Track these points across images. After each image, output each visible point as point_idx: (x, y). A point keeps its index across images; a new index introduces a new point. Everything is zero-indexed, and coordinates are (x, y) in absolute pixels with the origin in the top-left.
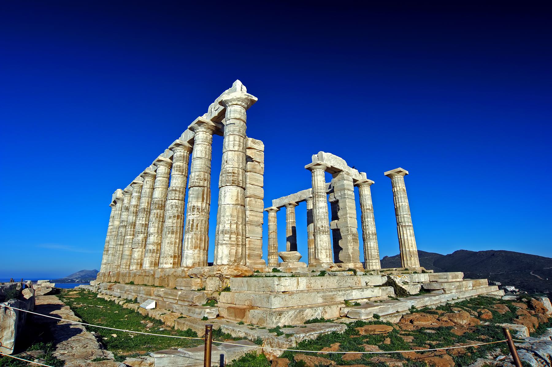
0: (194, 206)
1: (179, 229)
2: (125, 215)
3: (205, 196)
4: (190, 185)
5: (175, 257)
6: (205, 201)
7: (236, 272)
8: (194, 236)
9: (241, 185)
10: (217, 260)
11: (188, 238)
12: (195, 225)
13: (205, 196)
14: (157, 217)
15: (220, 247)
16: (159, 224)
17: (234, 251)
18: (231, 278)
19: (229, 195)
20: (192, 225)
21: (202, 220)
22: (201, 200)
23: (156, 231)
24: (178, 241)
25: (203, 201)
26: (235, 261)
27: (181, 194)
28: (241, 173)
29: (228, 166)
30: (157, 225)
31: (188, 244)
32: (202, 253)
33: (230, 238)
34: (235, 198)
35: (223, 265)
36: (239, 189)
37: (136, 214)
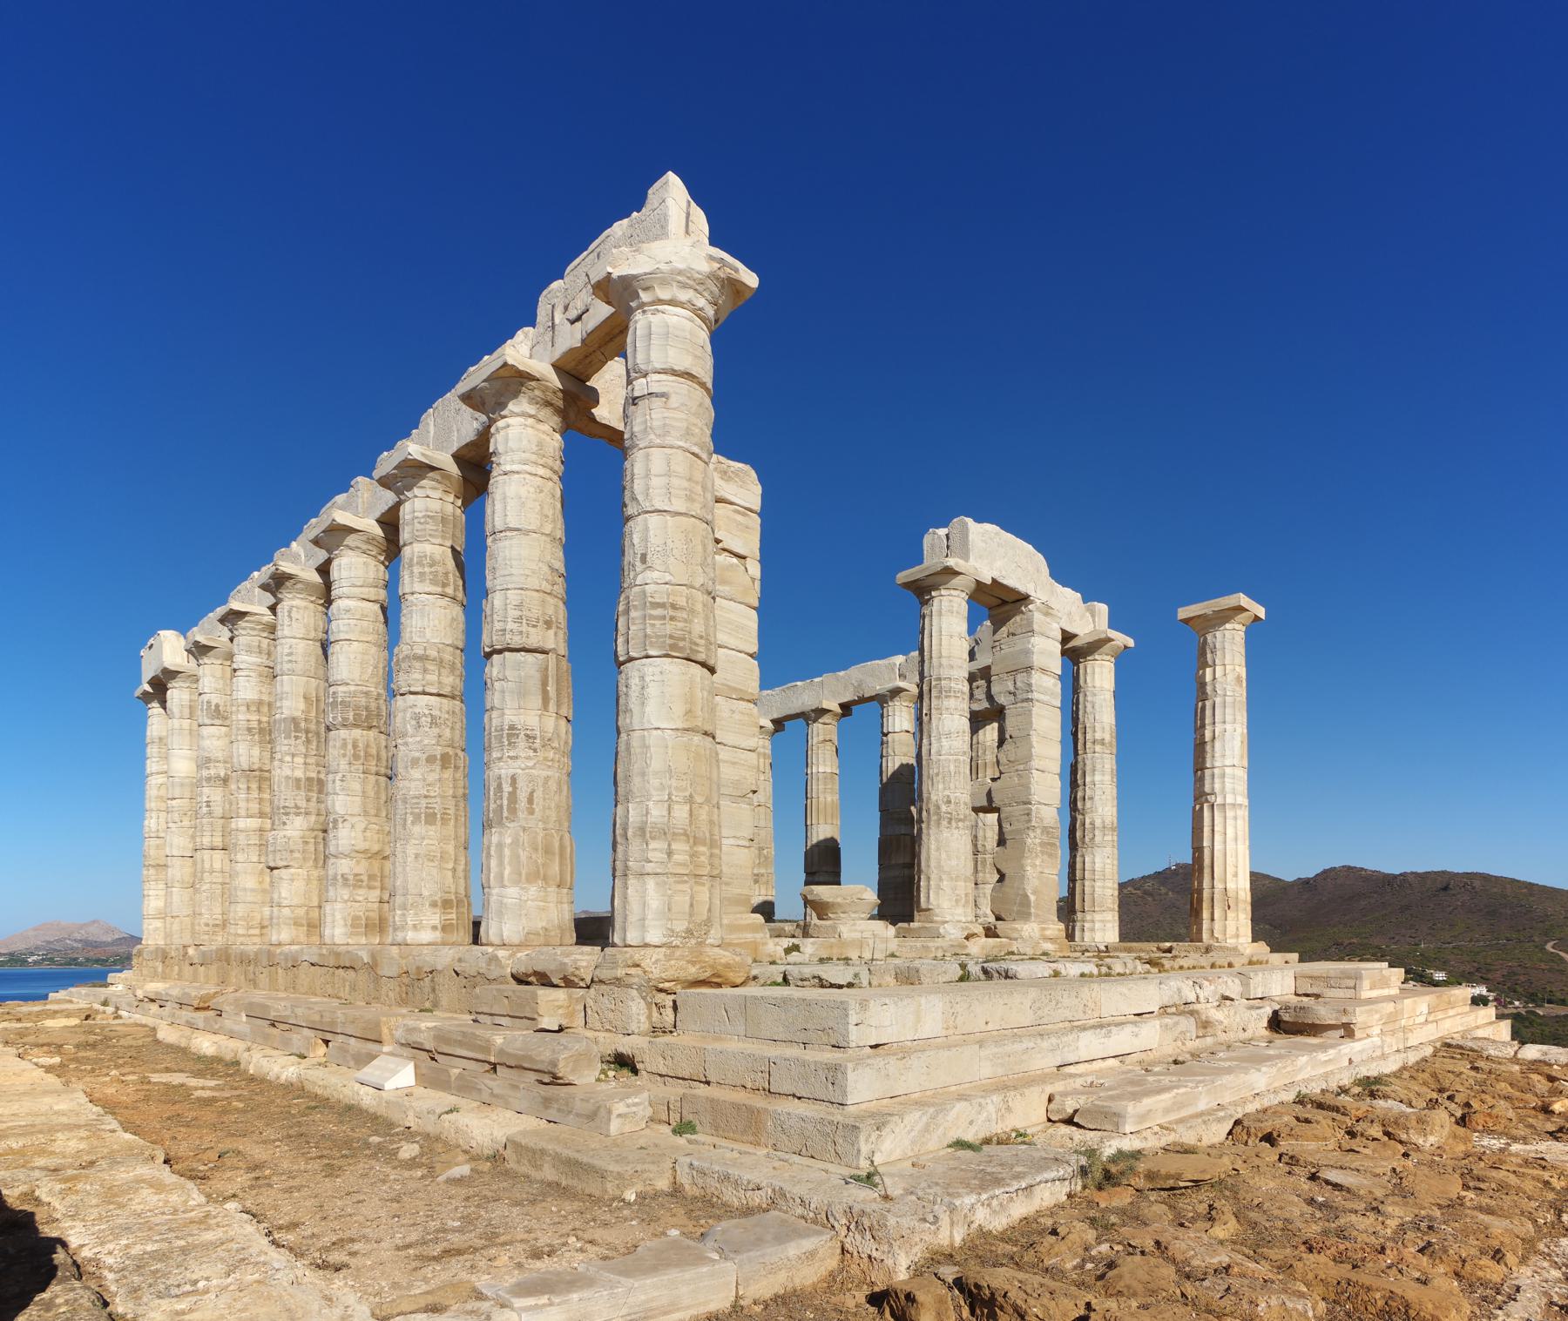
1: (451, 803)
2: (214, 739)
3: (551, 689)
4: (488, 639)
6: (552, 706)
7: (693, 972)
8: (524, 838)
9: (701, 657)
10: (624, 930)
11: (500, 845)
12: (522, 796)
13: (551, 689)
14: (356, 757)
15: (632, 881)
16: (364, 781)
17: (682, 901)
18: (678, 989)
19: (656, 693)
21: (547, 778)
22: (538, 701)
23: (357, 810)
24: (450, 848)
26: (689, 932)
27: (445, 672)
28: (699, 607)
30: (357, 786)
31: (501, 864)
32: (553, 897)
33: (670, 854)
34: (679, 709)
35: (646, 945)
36: (697, 670)
37: (266, 734)
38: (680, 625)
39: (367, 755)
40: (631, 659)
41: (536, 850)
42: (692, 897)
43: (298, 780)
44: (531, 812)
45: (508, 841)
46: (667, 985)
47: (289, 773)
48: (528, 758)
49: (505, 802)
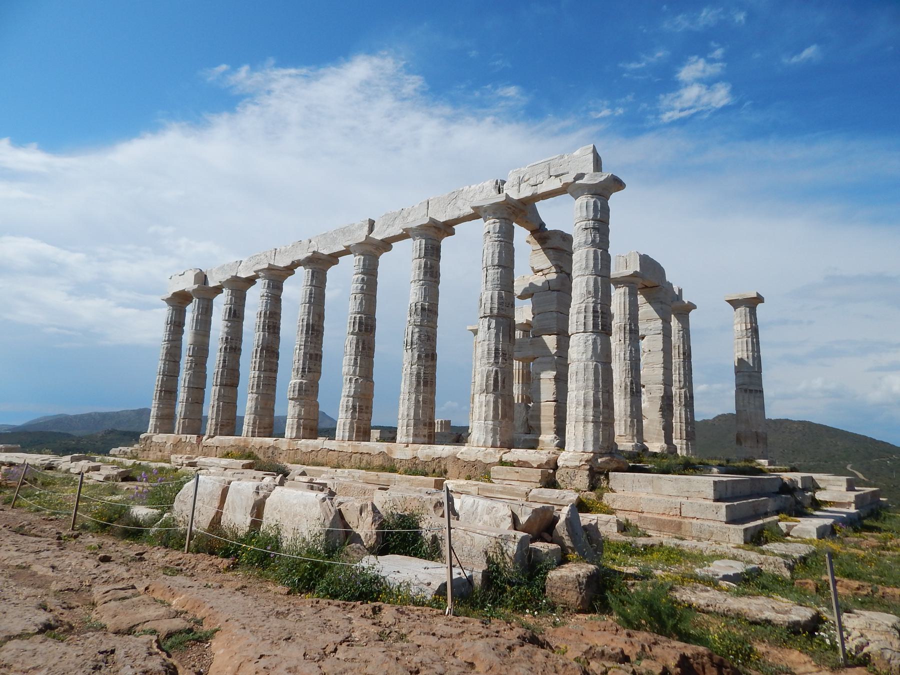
0: (497, 350)
14: (363, 348)
43: (311, 355)
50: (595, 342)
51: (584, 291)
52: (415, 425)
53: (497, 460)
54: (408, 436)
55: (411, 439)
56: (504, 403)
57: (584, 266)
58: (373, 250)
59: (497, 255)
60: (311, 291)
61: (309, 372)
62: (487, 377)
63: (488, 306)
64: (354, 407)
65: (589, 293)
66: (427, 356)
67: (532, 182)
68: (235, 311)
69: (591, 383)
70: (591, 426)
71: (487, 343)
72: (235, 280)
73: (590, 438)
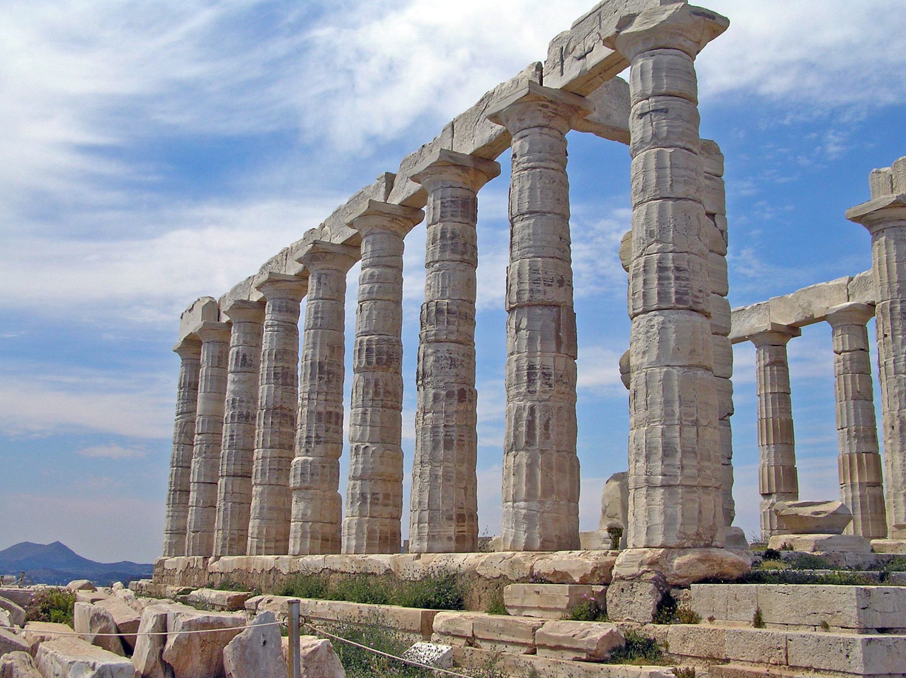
0: (531, 367)
5: (461, 518)
7: (703, 570)
14: (376, 393)
20: (531, 424)
21: (560, 408)
22: (553, 346)
23: (377, 438)
25: (558, 351)
29: (655, 247)
30: (378, 419)
38: (684, 283)
39: (387, 392)
40: (645, 312)
41: (551, 469)
42: (700, 505)
43: (320, 414)
44: (548, 438)
45: (529, 462)
46: (681, 581)
47: (313, 408)
48: (545, 392)
49: (524, 429)
50: (663, 329)
51: (643, 234)
52: (431, 520)
53: (526, 573)
54: (420, 539)
55: (425, 545)
56: (548, 467)
57: (640, 187)
58: (388, 225)
59: (526, 194)
60: (317, 307)
61: (317, 443)
62: (518, 419)
63: (515, 288)
64: (363, 495)
65: (651, 234)
66: (449, 395)
67: (578, 53)
68: (244, 356)
69: (657, 410)
70: (659, 493)
71: (515, 357)
72: (241, 306)
73: (658, 519)
